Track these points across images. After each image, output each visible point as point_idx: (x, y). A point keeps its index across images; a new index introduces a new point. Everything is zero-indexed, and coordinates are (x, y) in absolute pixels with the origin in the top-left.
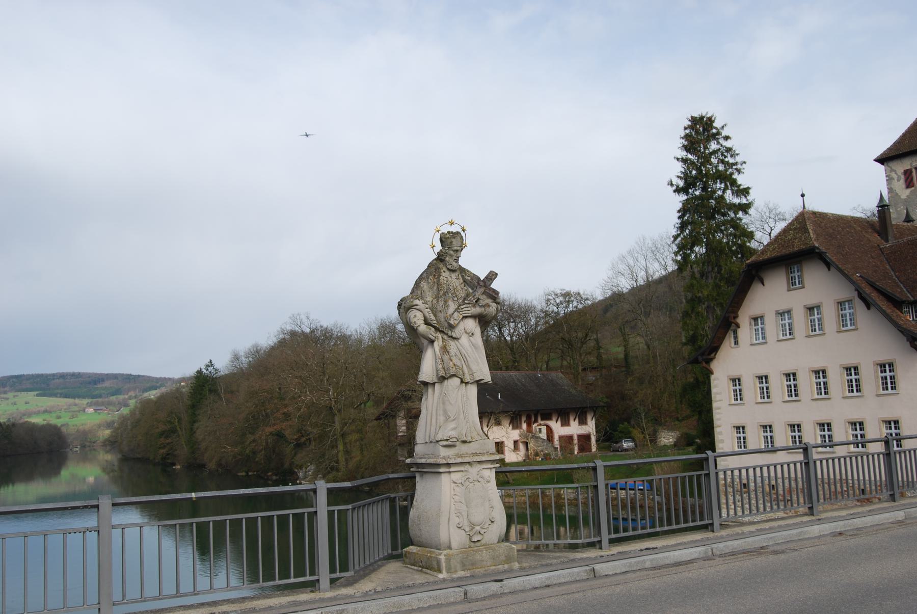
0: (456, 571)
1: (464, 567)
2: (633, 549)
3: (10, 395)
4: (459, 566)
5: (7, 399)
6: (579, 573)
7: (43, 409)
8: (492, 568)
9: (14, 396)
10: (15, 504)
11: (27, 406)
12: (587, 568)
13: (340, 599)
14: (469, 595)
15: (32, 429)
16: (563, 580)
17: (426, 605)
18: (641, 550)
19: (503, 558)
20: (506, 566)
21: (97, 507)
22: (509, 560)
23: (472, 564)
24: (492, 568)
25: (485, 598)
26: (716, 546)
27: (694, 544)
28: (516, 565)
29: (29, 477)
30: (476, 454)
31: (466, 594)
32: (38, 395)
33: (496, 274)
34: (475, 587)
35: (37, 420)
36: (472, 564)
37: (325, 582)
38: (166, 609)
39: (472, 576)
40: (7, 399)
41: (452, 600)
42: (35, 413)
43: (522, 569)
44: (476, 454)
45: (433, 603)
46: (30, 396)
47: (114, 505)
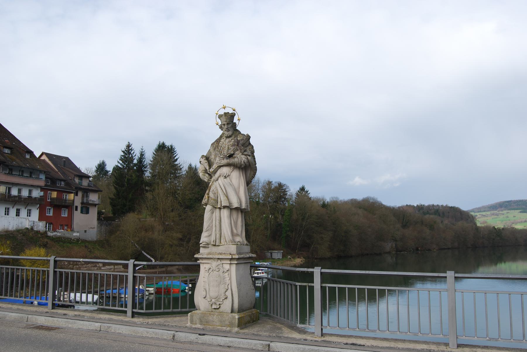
0: (196, 324)
1: (201, 323)
2: (339, 341)
3: (505, 212)
4: (198, 321)
5: (503, 214)
6: (255, 345)
7: (524, 220)
8: (219, 327)
9: (507, 213)
10: (511, 274)
11: (515, 218)
12: (264, 343)
13: (130, 323)
14: (175, 337)
15: (514, 232)
16: (242, 346)
17: (150, 336)
18: (347, 344)
19: (227, 323)
20: (228, 329)
21: (446, 277)
22: (231, 325)
23: (207, 322)
24: (219, 327)
25: (184, 343)
26: (30, 316)
27: (18, 311)
28: (236, 329)
29: (514, 259)
30: (221, 254)
31: (174, 336)
32: (520, 212)
33: (103, 161)
34: (279, 344)
35: (519, 227)
36: (207, 322)
37: (129, 313)
38: (398, 340)
39: (203, 329)
40: (503, 214)
41: (165, 337)
42: (519, 223)
43: (237, 333)
44: (221, 254)
45: (154, 336)
46: (516, 213)
47: (455, 277)
